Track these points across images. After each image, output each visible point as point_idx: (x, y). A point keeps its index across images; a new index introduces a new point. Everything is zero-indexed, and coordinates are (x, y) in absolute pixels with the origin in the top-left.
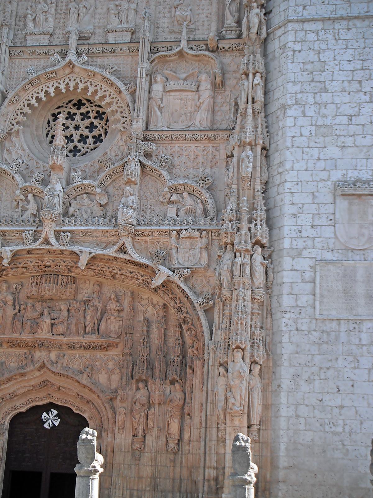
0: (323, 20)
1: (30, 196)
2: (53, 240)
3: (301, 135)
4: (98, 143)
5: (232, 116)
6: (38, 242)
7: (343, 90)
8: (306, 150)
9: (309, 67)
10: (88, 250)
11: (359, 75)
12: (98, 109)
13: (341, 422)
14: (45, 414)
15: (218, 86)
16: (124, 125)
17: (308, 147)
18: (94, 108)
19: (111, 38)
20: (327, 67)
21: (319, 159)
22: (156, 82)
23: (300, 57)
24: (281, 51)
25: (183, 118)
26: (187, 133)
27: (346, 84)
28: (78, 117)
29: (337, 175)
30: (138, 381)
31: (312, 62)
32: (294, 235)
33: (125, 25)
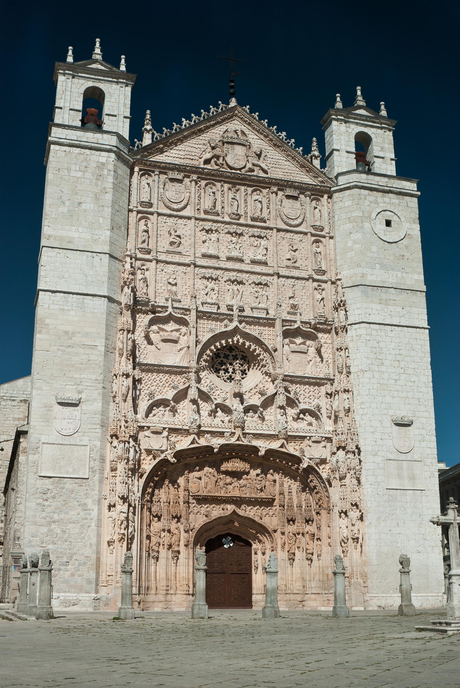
0: (379, 324)
1: (218, 409)
2: (243, 439)
4: (244, 376)
8: (376, 397)
9: (374, 350)
10: (264, 446)
11: (399, 358)
12: (243, 354)
13: (400, 541)
14: (224, 539)
21: (382, 402)
24: (358, 338)
25: (300, 368)
27: (392, 362)
29: (391, 412)
30: (289, 521)
32: (373, 443)
33: (262, 305)
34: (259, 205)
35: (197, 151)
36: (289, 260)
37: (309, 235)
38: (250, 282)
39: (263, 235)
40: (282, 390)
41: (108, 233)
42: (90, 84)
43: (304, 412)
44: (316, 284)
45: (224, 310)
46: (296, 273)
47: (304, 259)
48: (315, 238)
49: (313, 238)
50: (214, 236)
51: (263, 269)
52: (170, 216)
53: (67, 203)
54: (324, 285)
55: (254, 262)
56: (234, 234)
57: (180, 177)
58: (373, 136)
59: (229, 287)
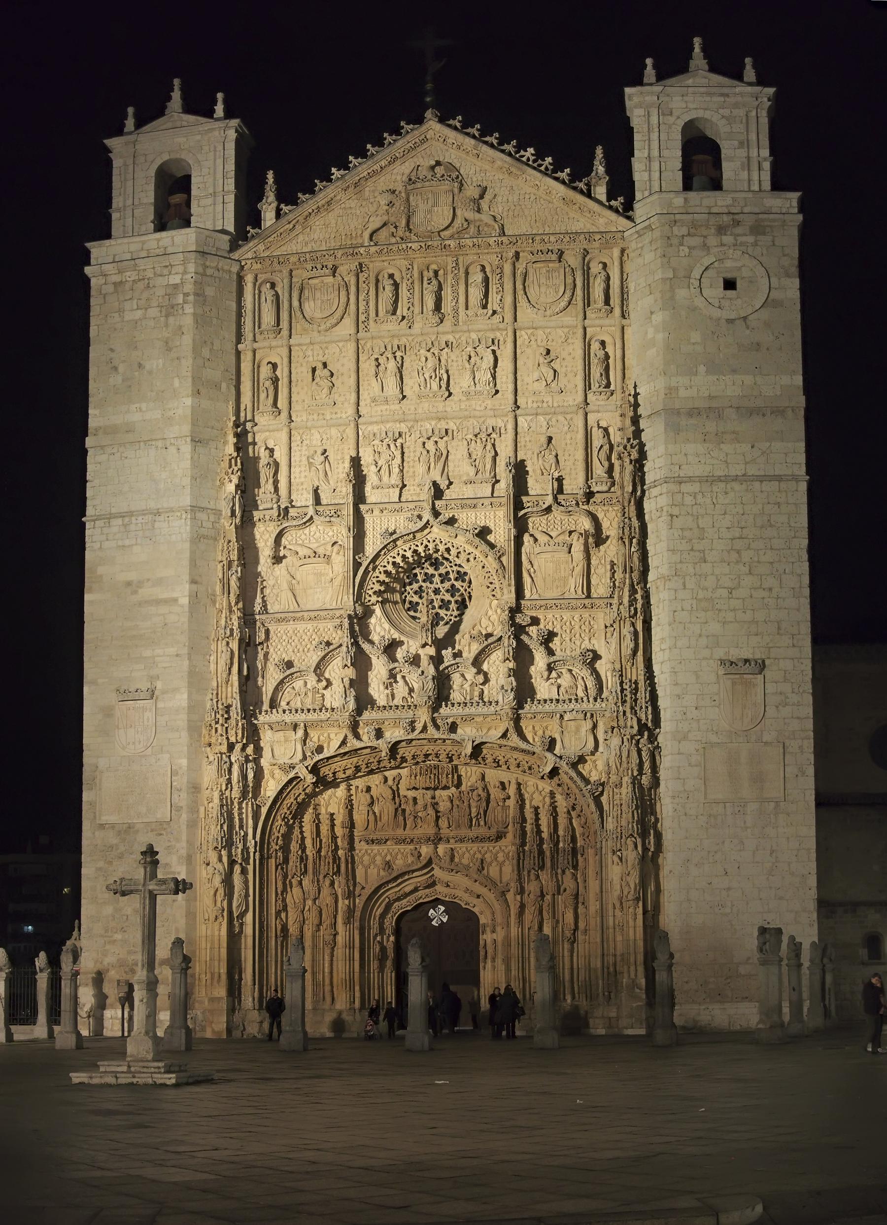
3: (683, 610)
5: (609, 581)
6: (417, 732)
7: (723, 561)
9: (687, 534)
12: (459, 569)
16: (494, 593)
17: (690, 622)
18: (455, 568)
20: (706, 535)
21: (700, 636)
23: (678, 523)
24: (658, 514)
26: (562, 601)
28: (437, 579)
29: (720, 653)
31: (691, 529)
41: (188, 401)
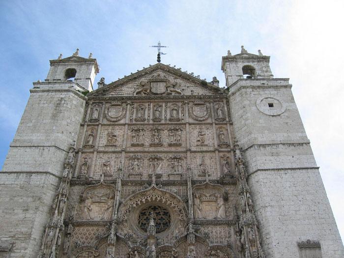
1: (136, 252)
12: (164, 211)
15: (226, 199)
19: (172, 178)
22: (196, 197)
27: (291, 197)
33: (178, 173)
34: (175, 112)
35: (133, 89)
36: (199, 141)
37: (214, 125)
38: (168, 158)
39: (178, 128)
40: (191, 230)
42: (69, 67)
43: (213, 248)
44: (221, 154)
45: (145, 178)
46: (205, 149)
47: (211, 140)
48: (220, 126)
49: (217, 126)
50: (141, 133)
51: (179, 149)
52: (109, 125)
53: (33, 121)
54: (228, 155)
55: (170, 145)
56: (156, 131)
57: (119, 103)
58: (254, 66)
59: (151, 163)
